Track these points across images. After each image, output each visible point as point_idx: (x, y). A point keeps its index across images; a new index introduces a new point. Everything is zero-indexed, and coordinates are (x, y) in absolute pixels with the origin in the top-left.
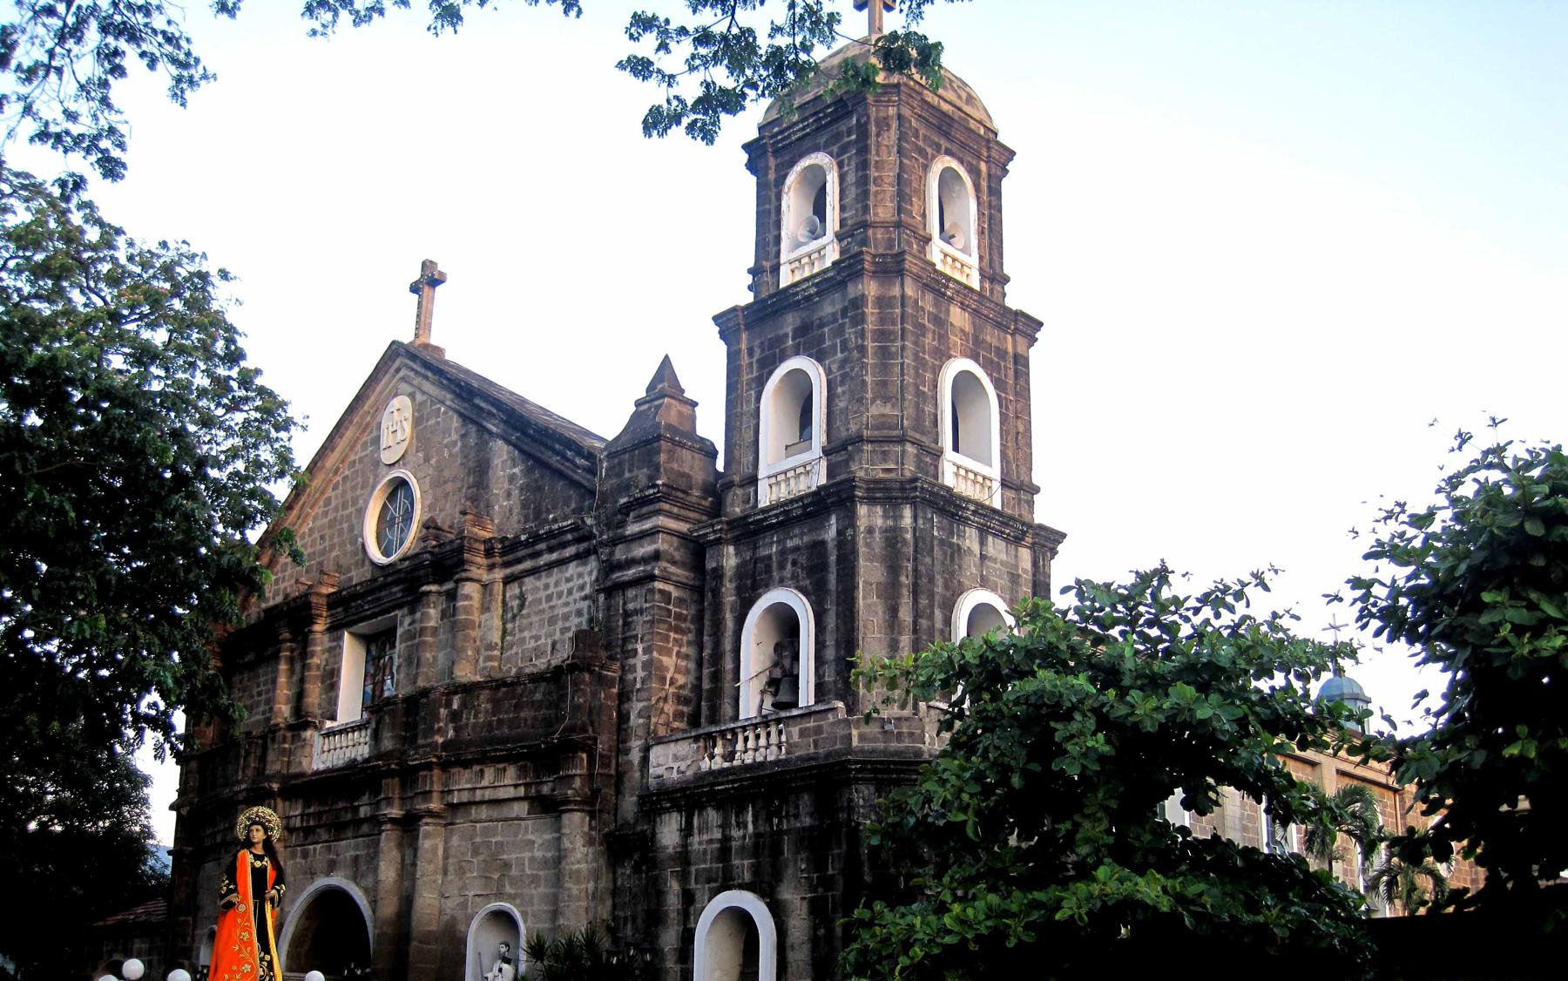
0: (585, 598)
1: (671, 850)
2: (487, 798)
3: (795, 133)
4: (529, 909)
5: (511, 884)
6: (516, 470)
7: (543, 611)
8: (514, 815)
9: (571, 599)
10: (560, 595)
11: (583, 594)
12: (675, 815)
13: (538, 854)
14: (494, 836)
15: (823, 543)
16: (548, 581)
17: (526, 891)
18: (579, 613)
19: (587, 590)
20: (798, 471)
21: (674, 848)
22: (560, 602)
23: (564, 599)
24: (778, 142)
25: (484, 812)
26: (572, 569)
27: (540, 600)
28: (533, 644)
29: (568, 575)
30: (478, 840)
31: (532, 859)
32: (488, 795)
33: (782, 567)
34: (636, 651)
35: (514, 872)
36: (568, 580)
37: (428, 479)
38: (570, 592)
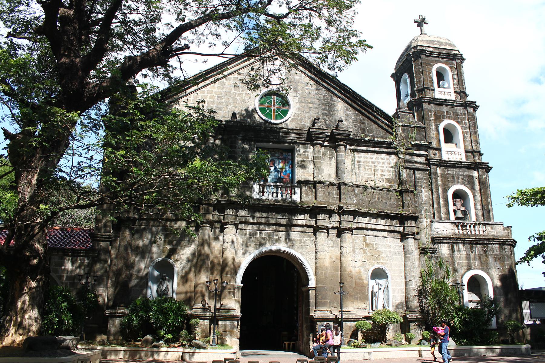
0: (392, 167)
1: (446, 255)
2: (373, 228)
3: (435, 54)
4: (390, 268)
5: (383, 260)
6: (350, 113)
7: (369, 166)
8: (382, 235)
9: (383, 165)
10: (379, 163)
11: (390, 166)
12: (446, 245)
13: (393, 250)
14: (374, 241)
15: (472, 177)
16: (373, 156)
17: (388, 262)
18: (389, 171)
19: (392, 165)
20: (456, 153)
21: (447, 254)
22: (379, 165)
23: (381, 165)
24: (429, 54)
25: (369, 232)
26: (383, 156)
27: (368, 162)
28: (366, 175)
29: (381, 157)
30: (368, 242)
31: (390, 252)
32: (373, 227)
33: (458, 178)
34: (422, 192)
35: (383, 255)
36: (382, 159)
37: (297, 98)
38: (384, 163)
